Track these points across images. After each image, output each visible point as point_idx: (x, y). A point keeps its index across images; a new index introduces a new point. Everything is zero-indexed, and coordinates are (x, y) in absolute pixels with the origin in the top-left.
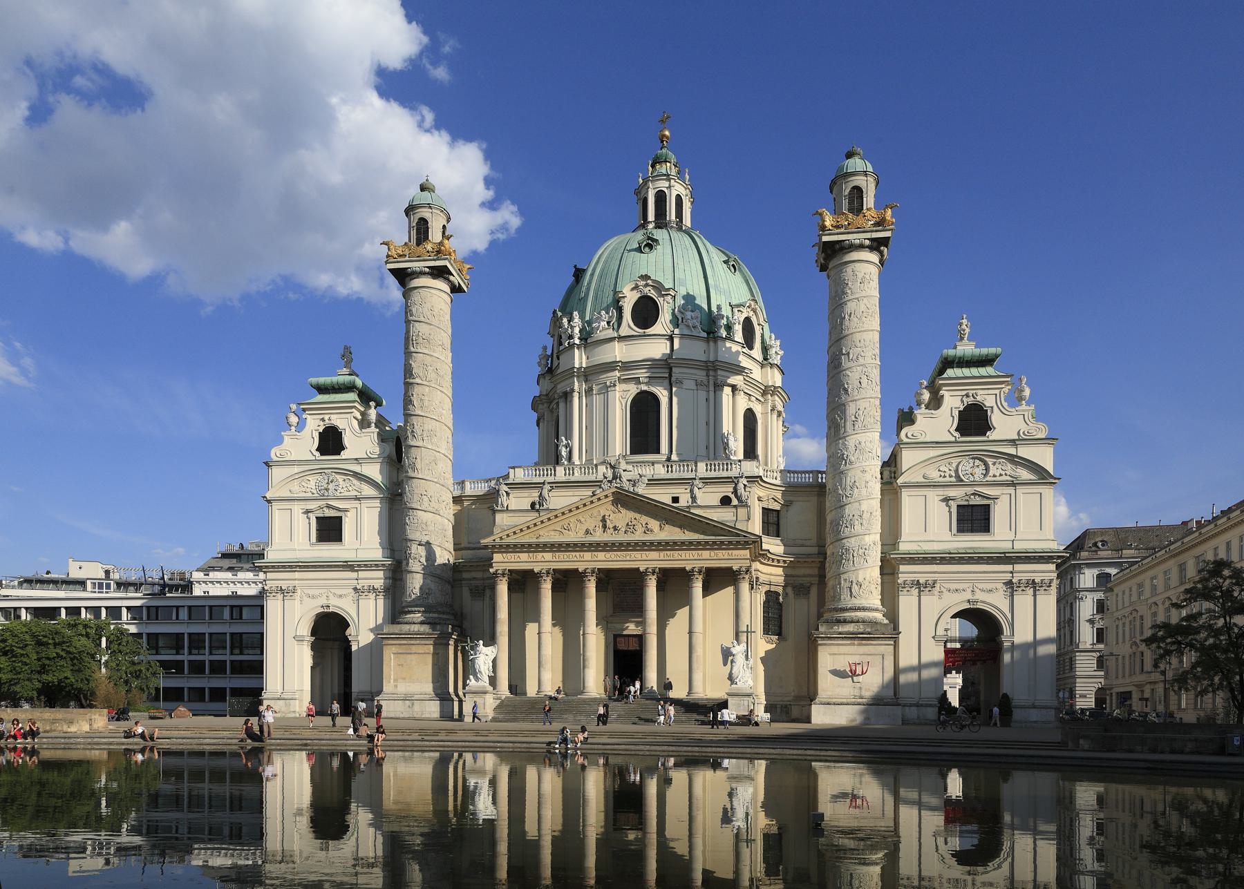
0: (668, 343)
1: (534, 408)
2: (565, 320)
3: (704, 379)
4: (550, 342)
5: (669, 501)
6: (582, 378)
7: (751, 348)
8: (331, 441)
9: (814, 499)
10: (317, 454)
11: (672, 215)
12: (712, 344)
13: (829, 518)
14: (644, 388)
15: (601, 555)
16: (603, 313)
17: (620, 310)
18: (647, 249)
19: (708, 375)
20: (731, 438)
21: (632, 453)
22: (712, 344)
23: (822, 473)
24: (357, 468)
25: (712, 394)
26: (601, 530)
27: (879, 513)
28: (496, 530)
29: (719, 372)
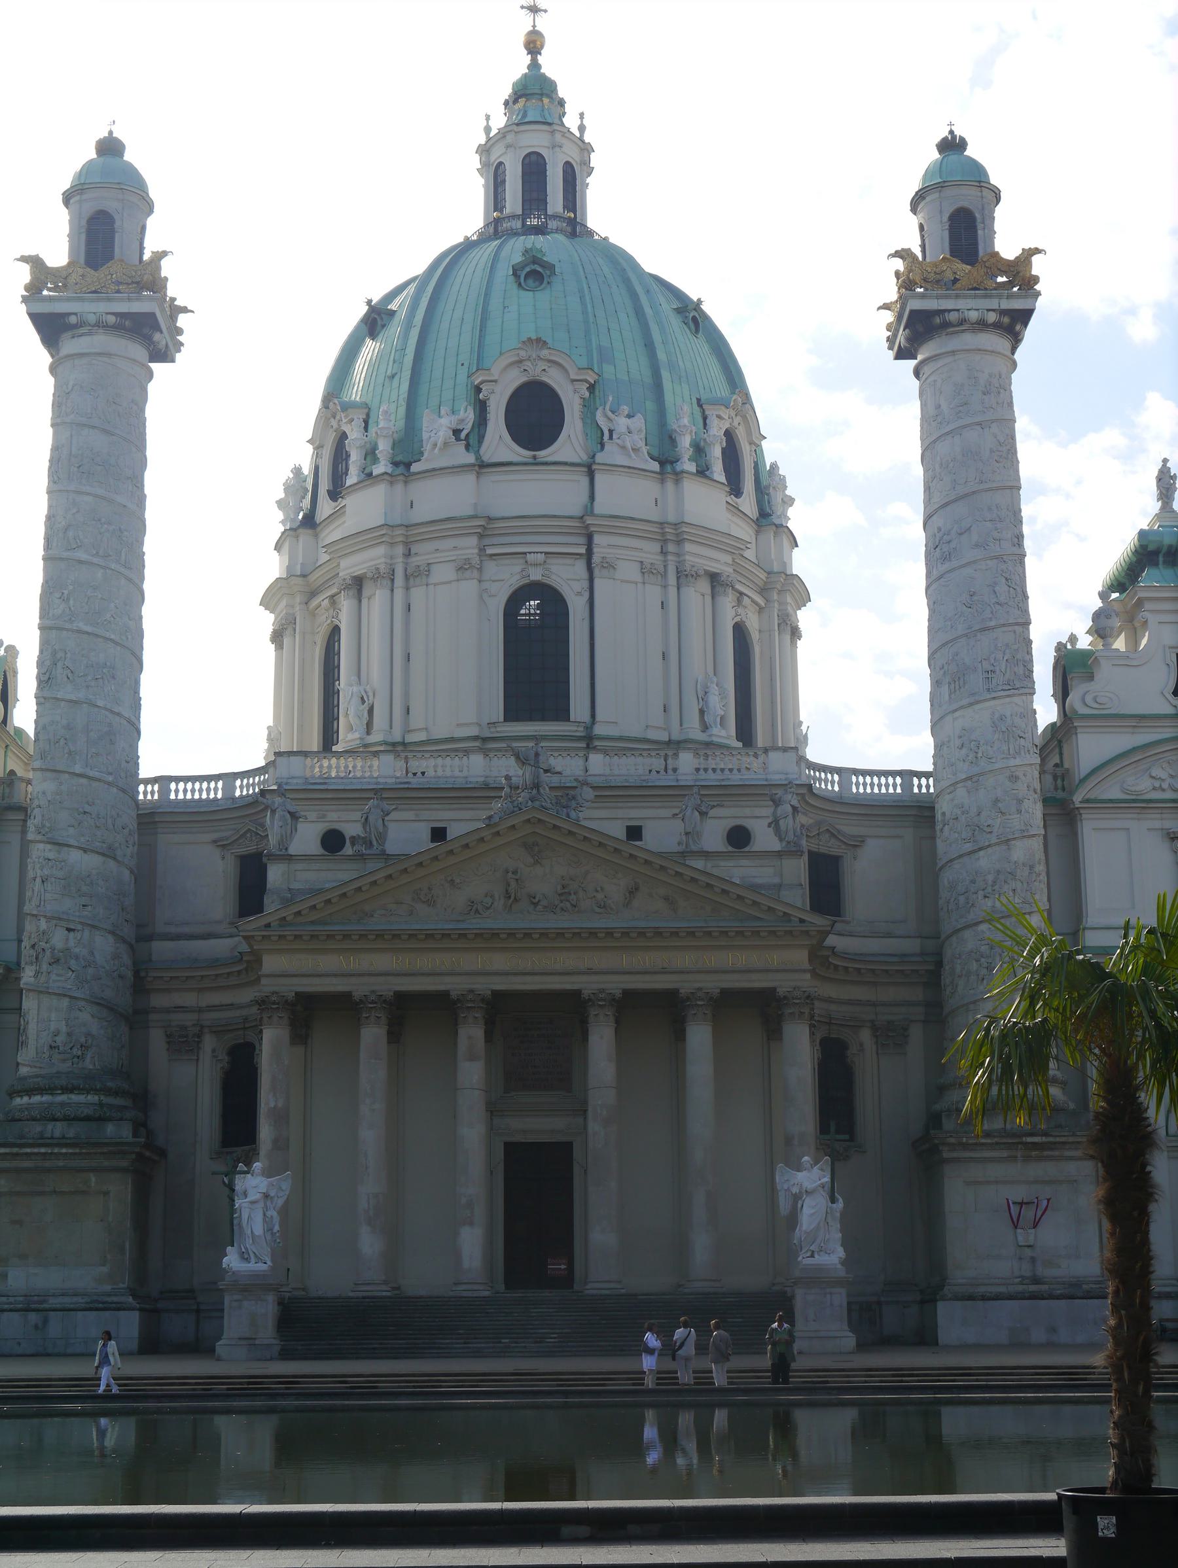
0: (585, 481)
1: (268, 601)
2: (359, 422)
3: (657, 559)
4: (304, 457)
5: (621, 834)
6: (400, 550)
7: (736, 491)
11: (555, 201)
12: (670, 485)
13: (946, 877)
14: (536, 575)
15: (499, 961)
17: (482, 408)
18: (530, 282)
19: (663, 552)
20: (714, 689)
21: (505, 720)
22: (670, 485)
23: (927, 775)
25: (672, 591)
27: (1041, 868)
28: (271, 904)
29: (688, 547)
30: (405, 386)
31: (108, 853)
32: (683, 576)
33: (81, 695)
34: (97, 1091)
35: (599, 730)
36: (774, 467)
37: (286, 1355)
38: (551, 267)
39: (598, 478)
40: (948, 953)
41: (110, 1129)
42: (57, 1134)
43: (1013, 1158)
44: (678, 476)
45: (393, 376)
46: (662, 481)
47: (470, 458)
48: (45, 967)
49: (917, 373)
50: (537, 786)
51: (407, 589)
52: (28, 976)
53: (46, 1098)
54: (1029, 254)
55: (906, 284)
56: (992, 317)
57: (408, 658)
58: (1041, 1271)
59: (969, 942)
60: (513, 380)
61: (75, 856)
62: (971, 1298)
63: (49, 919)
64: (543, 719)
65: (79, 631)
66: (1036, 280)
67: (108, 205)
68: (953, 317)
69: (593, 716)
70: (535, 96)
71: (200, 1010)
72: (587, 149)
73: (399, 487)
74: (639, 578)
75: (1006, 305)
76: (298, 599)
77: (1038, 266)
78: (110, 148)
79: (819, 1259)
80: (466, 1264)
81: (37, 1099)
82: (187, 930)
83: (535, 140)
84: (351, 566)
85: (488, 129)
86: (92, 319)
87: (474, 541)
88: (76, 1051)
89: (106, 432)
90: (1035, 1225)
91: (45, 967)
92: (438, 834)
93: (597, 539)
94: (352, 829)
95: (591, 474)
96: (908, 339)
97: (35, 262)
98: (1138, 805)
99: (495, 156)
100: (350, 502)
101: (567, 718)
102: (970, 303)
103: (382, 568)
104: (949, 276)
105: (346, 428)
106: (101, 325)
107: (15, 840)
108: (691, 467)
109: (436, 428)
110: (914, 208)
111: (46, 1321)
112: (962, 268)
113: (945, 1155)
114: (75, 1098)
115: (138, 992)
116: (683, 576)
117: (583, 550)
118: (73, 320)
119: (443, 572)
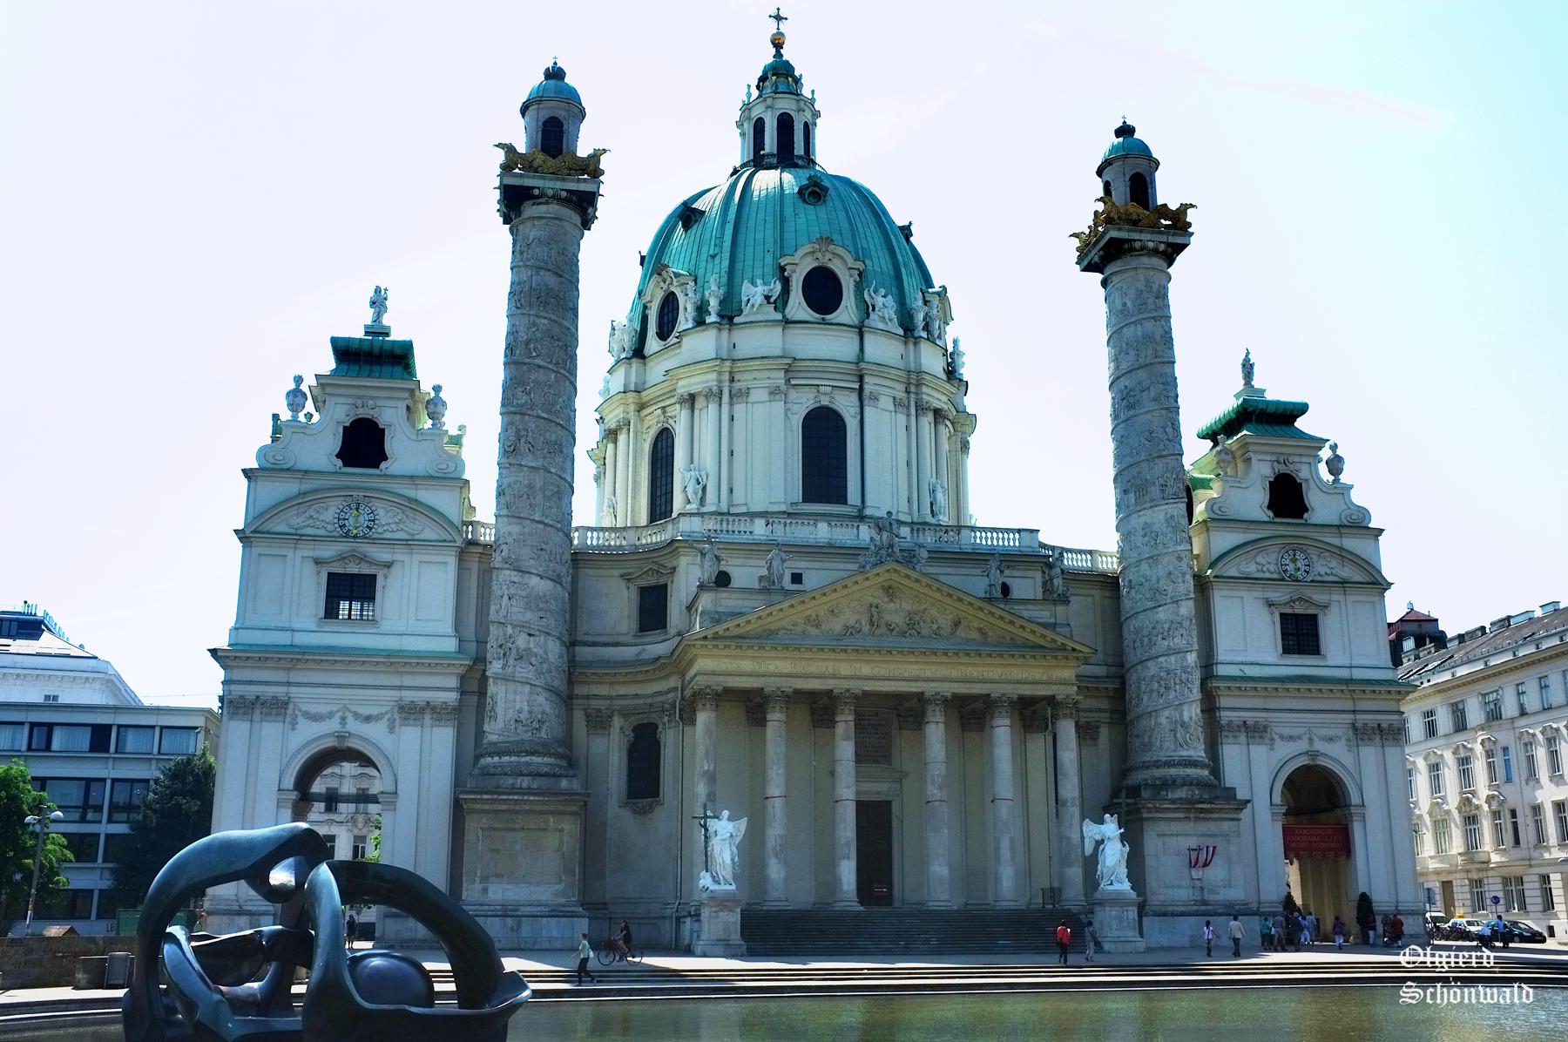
0: (857, 338)
3: (901, 395)
6: (726, 377)
8: (363, 444)
9: (1097, 593)
10: (339, 463)
11: (799, 149)
13: (1132, 624)
14: (825, 401)
16: (759, 282)
17: (786, 283)
19: (908, 392)
20: (939, 489)
22: (911, 346)
24: (411, 493)
25: (913, 418)
26: (866, 628)
30: (726, 264)
31: (557, 580)
32: (921, 408)
33: (539, 463)
34: (550, 755)
35: (868, 512)
36: (955, 342)
37: (752, 953)
38: (826, 189)
39: (866, 336)
40: (1132, 678)
41: (564, 783)
42: (525, 785)
43: (1188, 818)
44: (917, 340)
45: (713, 257)
46: (906, 343)
47: (779, 316)
48: (511, 662)
49: (1104, 283)
50: (891, 546)
51: (731, 405)
52: (495, 667)
53: (513, 759)
54: (1184, 208)
55: (1105, 219)
56: (1162, 247)
57: (732, 453)
58: (1206, 896)
59: (1152, 668)
60: (808, 265)
61: (534, 581)
62: (1165, 914)
63: (514, 627)
64: (829, 502)
65: (538, 417)
66: (1189, 225)
67: (555, 114)
68: (1137, 245)
69: (863, 502)
70: (780, 76)
71: (611, 698)
72: (817, 114)
73: (725, 333)
74: (892, 408)
75: (1172, 240)
76: (632, 407)
77: (1191, 216)
78: (555, 74)
79: (1117, 886)
80: (845, 887)
81: (507, 759)
82: (601, 639)
83: (785, 104)
84: (685, 386)
85: (749, 95)
86: (550, 193)
87: (782, 374)
88: (536, 725)
89: (556, 274)
90: (1206, 865)
91: (511, 662)
92: (797, 578)
93: (867, 379)
94: (745, 574)
95: (861, 335)
96: (1101, 258)
97: (509, 149)
98: (1247, 579)
99: (756, 113)
100: (687, 342)
101: (845, 503)
102: (1149, 237)
103: (715, 389)
104: (1134, 217)
105: (678, 292)
106: (556, 198)
107: (474, 567)
108: (924, 334)
109: (754, 293)
110: (1100, 173)
111: (519, 924)
112: (1141, 210)
113: (1145, 815)
114: (535, 759)
115: (572, 681)
116: (921, 408)
117: (856, 386)
118: (536, 192)
119: (759, 395)
